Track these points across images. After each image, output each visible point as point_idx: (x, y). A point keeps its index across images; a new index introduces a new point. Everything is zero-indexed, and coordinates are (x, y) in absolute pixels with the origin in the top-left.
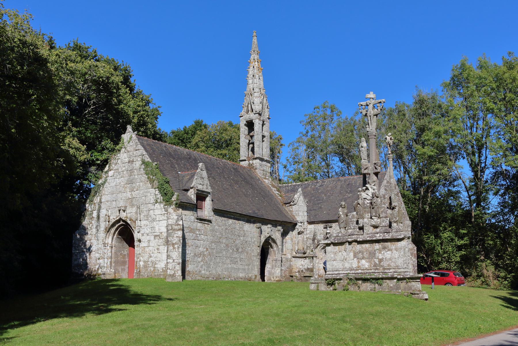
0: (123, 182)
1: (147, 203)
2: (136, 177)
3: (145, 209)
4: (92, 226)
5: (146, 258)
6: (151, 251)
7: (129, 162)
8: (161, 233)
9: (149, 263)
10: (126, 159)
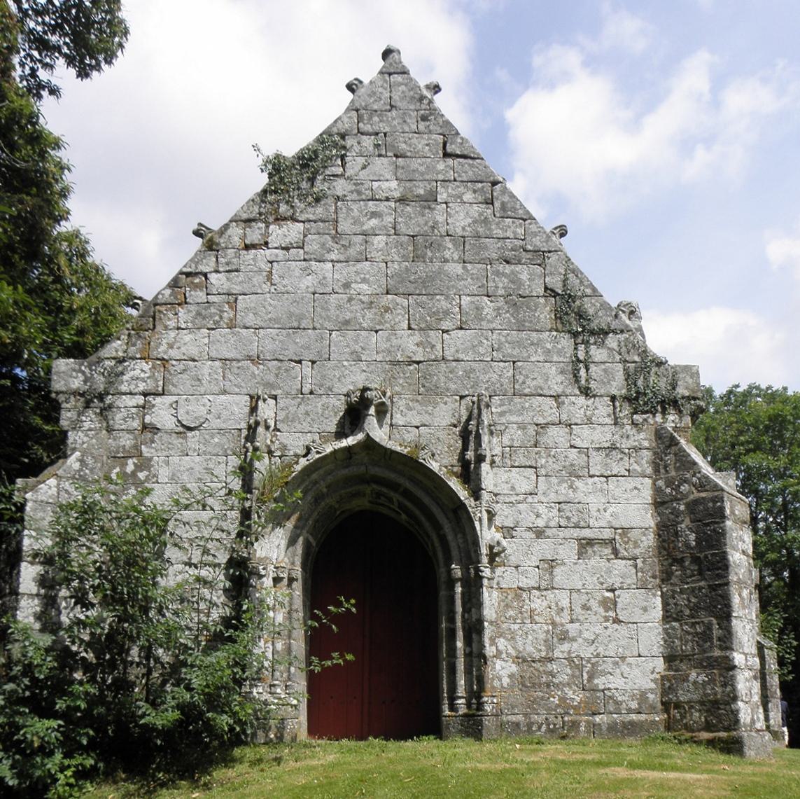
0: (364, 281)
1: (527, 391)
2: (458, 269)
3: (514, 418)
4: (138, 468)
5: (530, 648)
6: (566, 612)
7: (402, 200)
8: (625, 531)
9: (553, 667)
10: (385, 185)
